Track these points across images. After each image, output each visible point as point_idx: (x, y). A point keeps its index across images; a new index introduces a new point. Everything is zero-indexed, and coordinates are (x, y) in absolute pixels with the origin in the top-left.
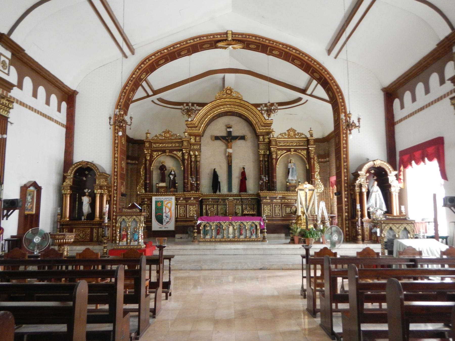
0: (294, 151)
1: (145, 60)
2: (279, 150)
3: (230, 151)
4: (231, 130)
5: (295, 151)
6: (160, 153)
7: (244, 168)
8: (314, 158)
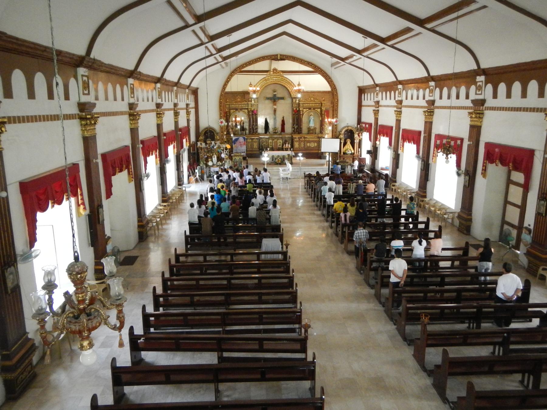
0: (313, 109)
1: (234, 71)
2: (304, 108)
3: (275, 107)
4: (276, 93)
5: (314, 109)
6: (234, 110)
7: (283, 118)
8: (324, 114)
